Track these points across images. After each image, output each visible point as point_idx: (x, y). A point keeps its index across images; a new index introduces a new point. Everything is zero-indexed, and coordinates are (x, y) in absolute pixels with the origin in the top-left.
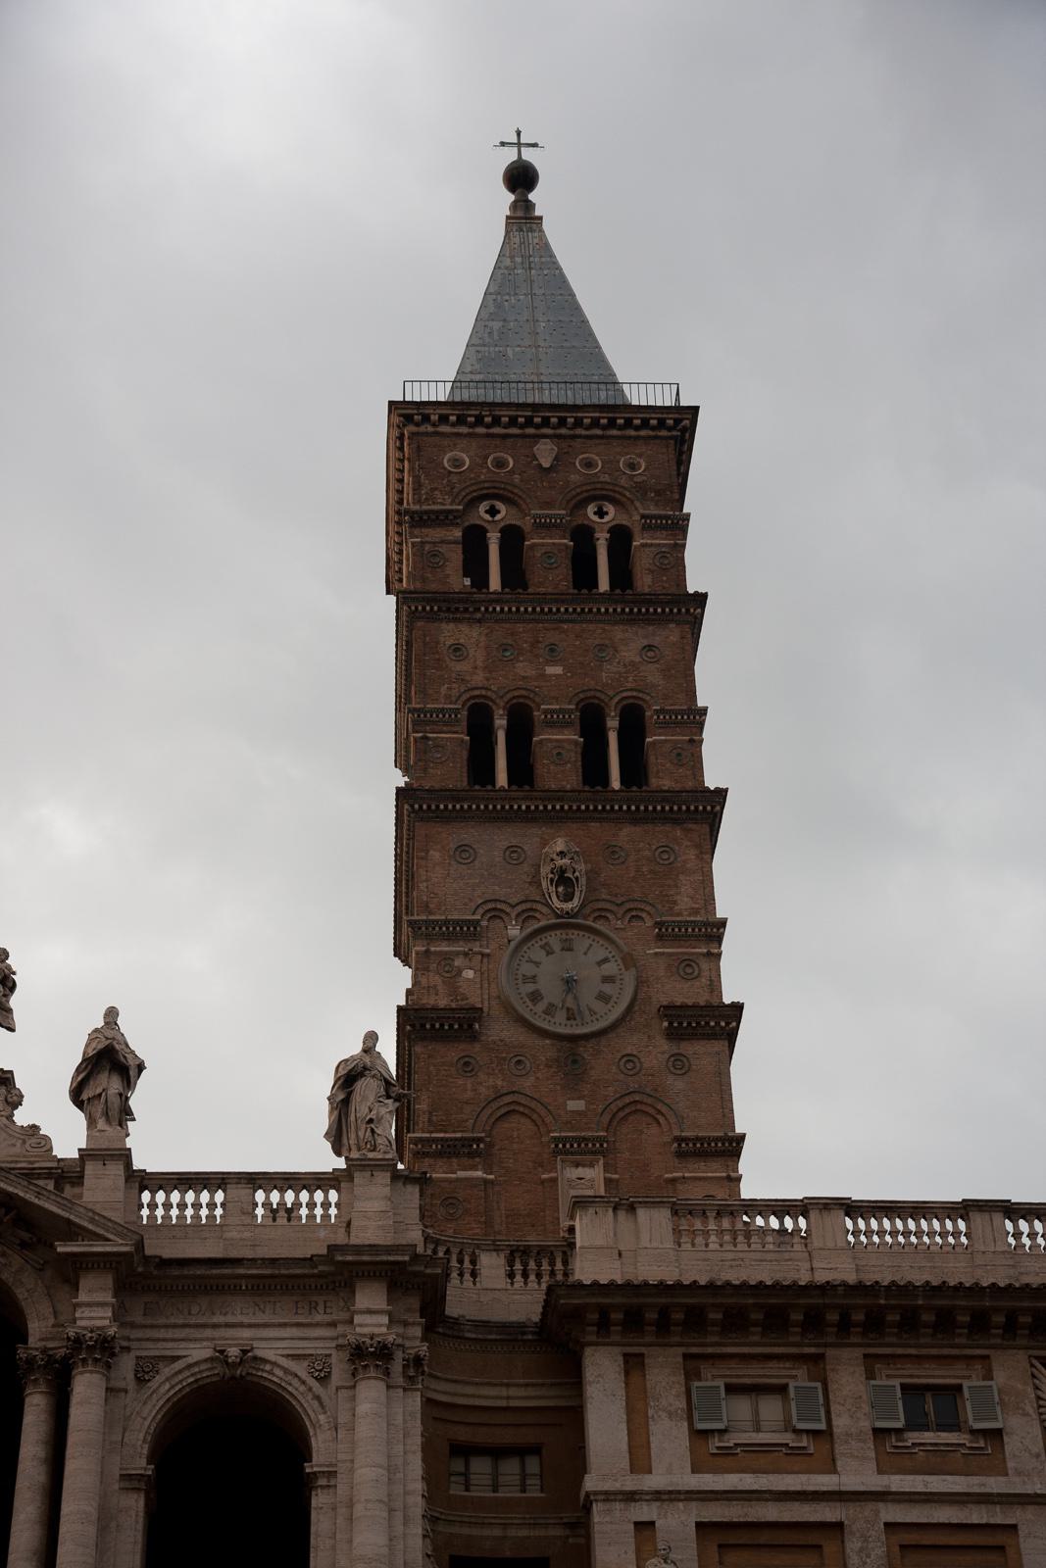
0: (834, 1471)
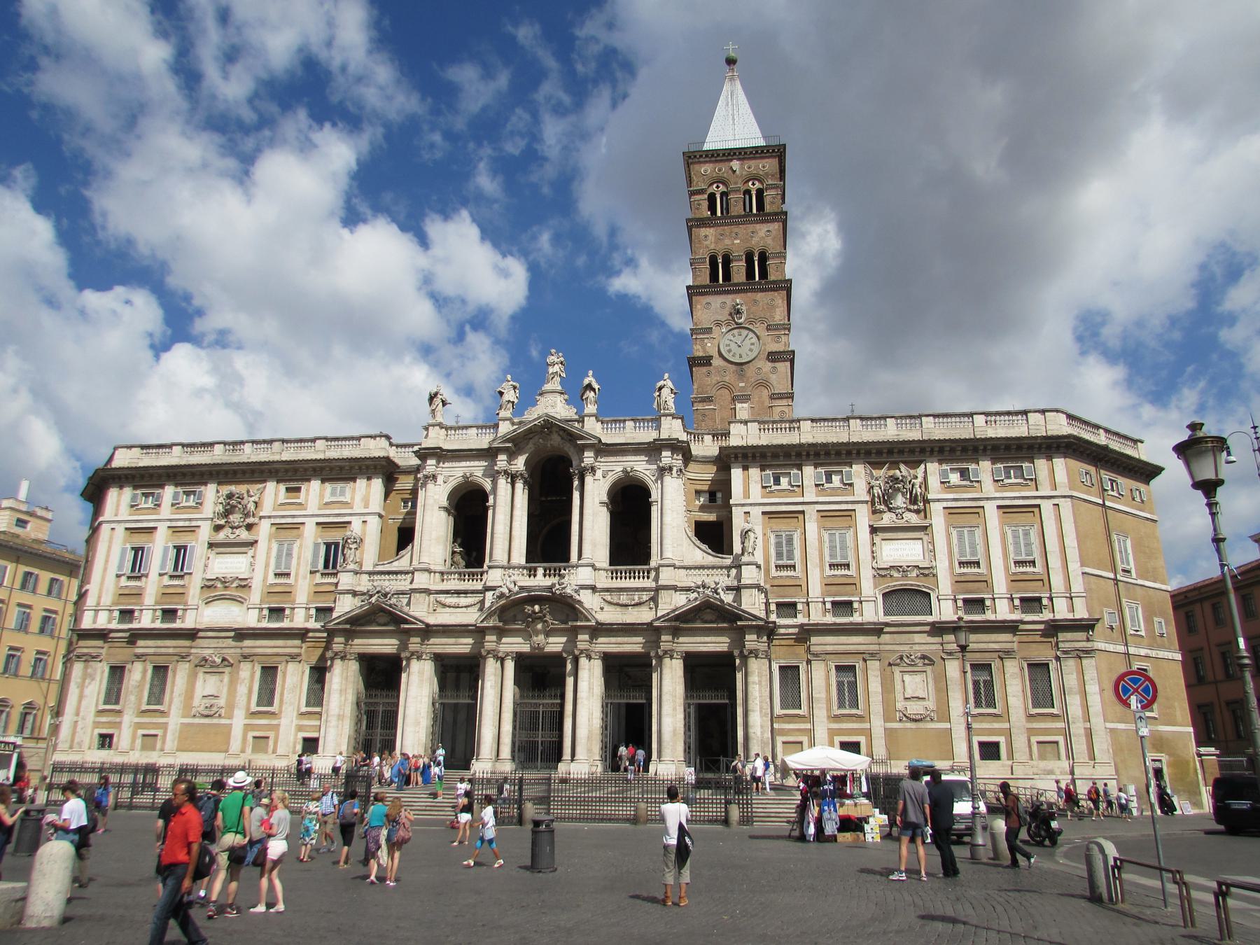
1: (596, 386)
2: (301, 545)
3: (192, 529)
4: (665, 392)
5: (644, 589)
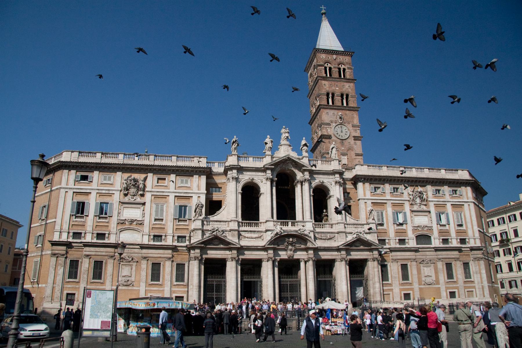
0: (385, 196)
1: (308, 145)
2: (167, 207)
3: (110, 195)
4: (334, 150)
5: (332, 233)
